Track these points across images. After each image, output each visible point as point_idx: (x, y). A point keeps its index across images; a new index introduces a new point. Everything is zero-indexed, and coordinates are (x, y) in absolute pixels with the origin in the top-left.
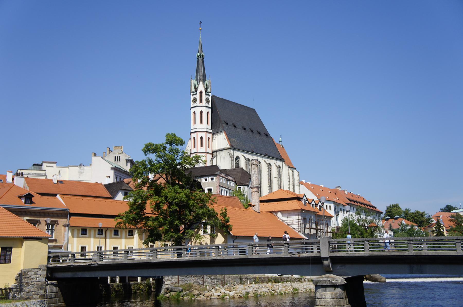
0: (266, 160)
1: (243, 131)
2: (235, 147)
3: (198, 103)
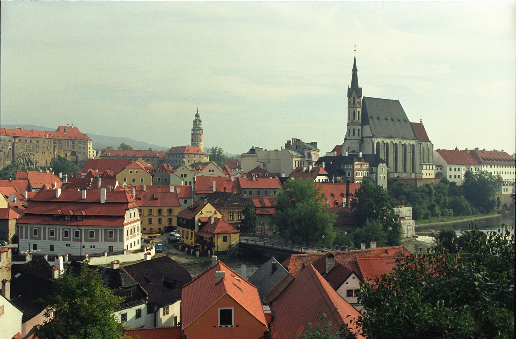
3: (352, 106)
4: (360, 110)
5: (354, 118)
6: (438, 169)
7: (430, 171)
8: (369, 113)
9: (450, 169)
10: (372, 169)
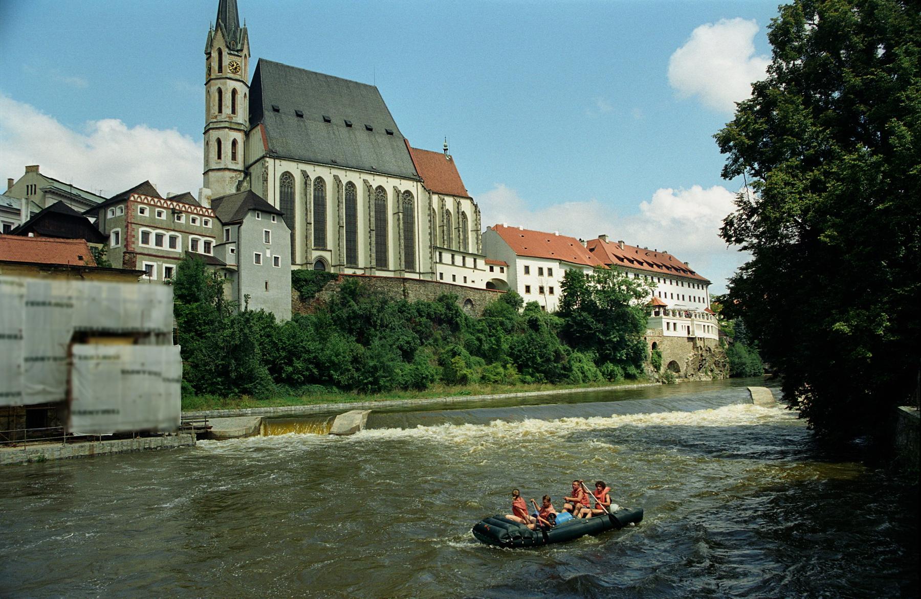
0: (369, 178)
1: (323, 125)
2: (282, 154)
4: (242, 90)
5: (220, 111)
6: (492, 269)
8: (268, 98)
10: (228, 231)
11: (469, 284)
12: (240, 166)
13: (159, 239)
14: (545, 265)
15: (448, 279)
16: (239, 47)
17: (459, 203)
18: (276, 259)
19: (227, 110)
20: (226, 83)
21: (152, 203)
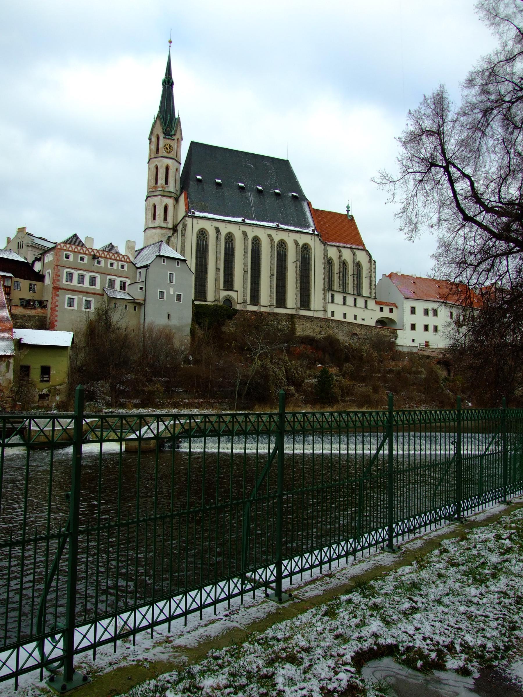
5: (156, 183)
6: (381, 309)
7: (361, 313)
9: (413, 311)
11: (359, 321)
12: (170, 225)
13: (81, 279)
14: (430, 306)
15: (339, 317)
16: (173, 133)
17: (354, 254)
18: (179, 296)
19: (161, 181)
20: (161, 161)
21: (76, 250)
